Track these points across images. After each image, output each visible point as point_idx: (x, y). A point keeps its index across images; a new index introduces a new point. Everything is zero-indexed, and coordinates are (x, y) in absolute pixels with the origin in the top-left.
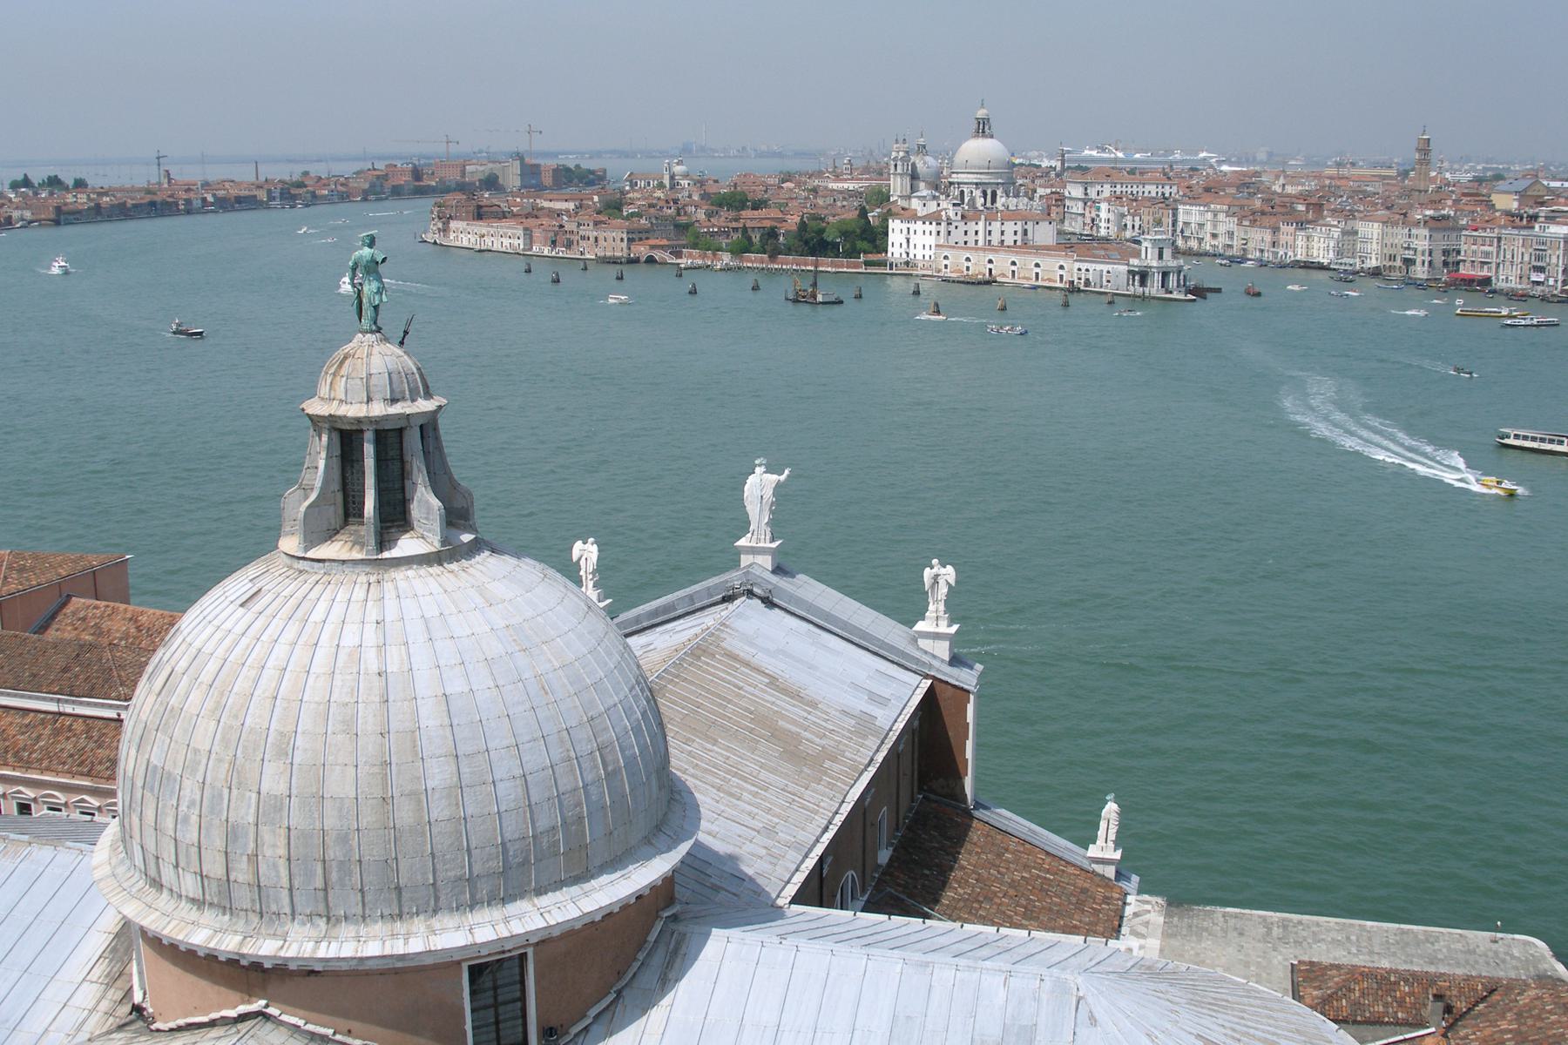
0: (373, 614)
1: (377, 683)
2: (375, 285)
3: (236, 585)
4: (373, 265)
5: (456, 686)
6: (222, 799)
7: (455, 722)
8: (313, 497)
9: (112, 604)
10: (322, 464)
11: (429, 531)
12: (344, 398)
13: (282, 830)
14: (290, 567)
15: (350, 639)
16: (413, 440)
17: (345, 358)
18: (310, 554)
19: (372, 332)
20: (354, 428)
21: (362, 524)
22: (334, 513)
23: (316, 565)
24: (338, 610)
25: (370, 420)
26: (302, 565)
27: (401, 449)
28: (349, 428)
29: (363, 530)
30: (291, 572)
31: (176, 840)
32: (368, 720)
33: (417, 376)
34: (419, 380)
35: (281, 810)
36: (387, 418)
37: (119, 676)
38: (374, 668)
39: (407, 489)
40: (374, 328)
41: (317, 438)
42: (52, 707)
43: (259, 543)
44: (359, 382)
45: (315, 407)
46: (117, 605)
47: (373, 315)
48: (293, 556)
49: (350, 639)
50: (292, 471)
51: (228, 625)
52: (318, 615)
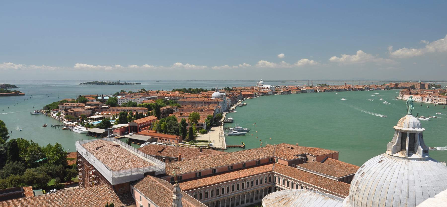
0: (406, 168)
1: (407, 181)
2: (412, 106)
3: (377, 158)
4: (411, 102)
5: (424, 185)
6: (372, 197)
7: (423, 192)
8: (395, 144)
9: (335, 160)
10: (397, 138)
11: (419, 154)
12: (403, 126)
13: (384, 205)
14: (388, 157)
15: (402, 172)
16: (418, 137)
17: (404, 119)
18: (393, 155)
19: (410, 115)
20: (405, 132)
21: (405, 151)
22: (399, 147)
23: (394, 157)
24: (399, 166)
25: (409, 131)
26: (391, 157)
27: (415, 138)
28: (404, 132)
29: (405, 152)
30: (389, 158)
31: (362, 203)
32: (405, 189)
33: (419, 124)
34: (420, 125)
35: (384, 201)
36: (412, 131)
37: (337, 173)
38: (406, 178)
39: (415, 145)
40: (411, 114)
41: (396, 134)
42: (325, 177)
43: (383, 151)
44: (407, 124)
45: (396, 127)
46: (336, 160)
47: (411, 111)
48: (390, 155)
49: (402, 172)
50: (390, 139)
51: (376, 165)
52: (395, 166)
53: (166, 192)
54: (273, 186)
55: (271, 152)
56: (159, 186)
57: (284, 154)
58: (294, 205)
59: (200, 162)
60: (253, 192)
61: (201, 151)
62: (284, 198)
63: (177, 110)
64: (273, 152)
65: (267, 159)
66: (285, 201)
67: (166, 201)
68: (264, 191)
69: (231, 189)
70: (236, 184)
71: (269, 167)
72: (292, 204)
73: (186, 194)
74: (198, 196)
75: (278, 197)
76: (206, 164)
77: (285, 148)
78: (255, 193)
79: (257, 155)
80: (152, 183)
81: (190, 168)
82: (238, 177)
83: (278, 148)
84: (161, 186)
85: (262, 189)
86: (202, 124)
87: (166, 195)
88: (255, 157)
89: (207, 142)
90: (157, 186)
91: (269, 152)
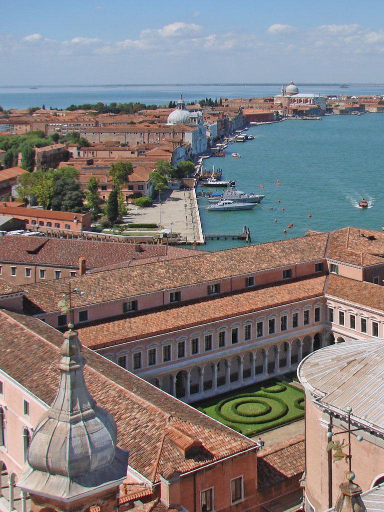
53: (47, 353)
54: (326, 331)
55: (320, 248)
56: (28, 339)
57: (352, 254)
58: (380, 377)
59: (136, 277)
60: (275, 348)
61: (141, 250)
62: (353, 359)
63: (79, 153)
64: (323, 248)
65: (309, 265)
66: (358, 367)
67: (46, 374)
68: (302, 343)
69: (215, 341)
70: (230, 328)
71: (316, 285)
72: (374, 374)
73: (98, 357)
74: (130, 360)
75: (338, 359)
76: (152, 282)
77: (353, 239)
78: (279, 350)
79: (284, 256)
80: (9, 329)
81: (110, 291)
82: (235, 311)
83: (335, 239)
84: (34, 336)
85: (299, 340)
86: (141, 184)
87: (45, 360)
88: (278, 263)
89: (154, 226)
90: (23, 338)
91: (315, 249)
